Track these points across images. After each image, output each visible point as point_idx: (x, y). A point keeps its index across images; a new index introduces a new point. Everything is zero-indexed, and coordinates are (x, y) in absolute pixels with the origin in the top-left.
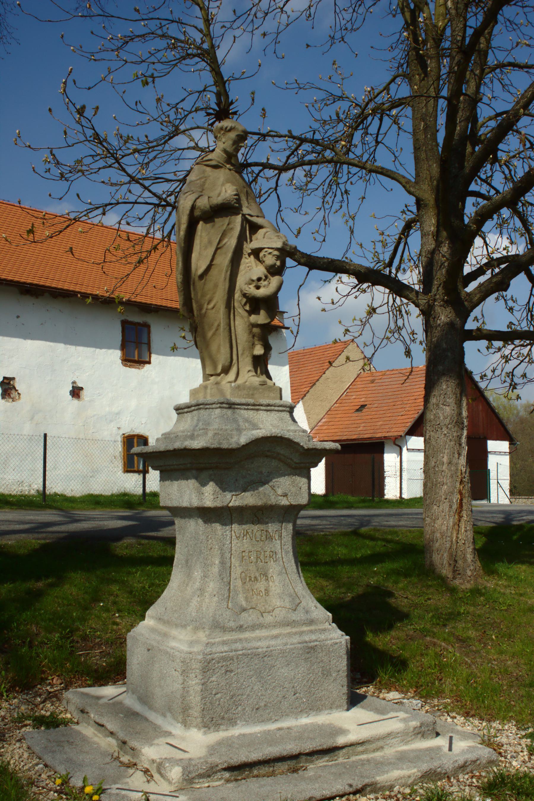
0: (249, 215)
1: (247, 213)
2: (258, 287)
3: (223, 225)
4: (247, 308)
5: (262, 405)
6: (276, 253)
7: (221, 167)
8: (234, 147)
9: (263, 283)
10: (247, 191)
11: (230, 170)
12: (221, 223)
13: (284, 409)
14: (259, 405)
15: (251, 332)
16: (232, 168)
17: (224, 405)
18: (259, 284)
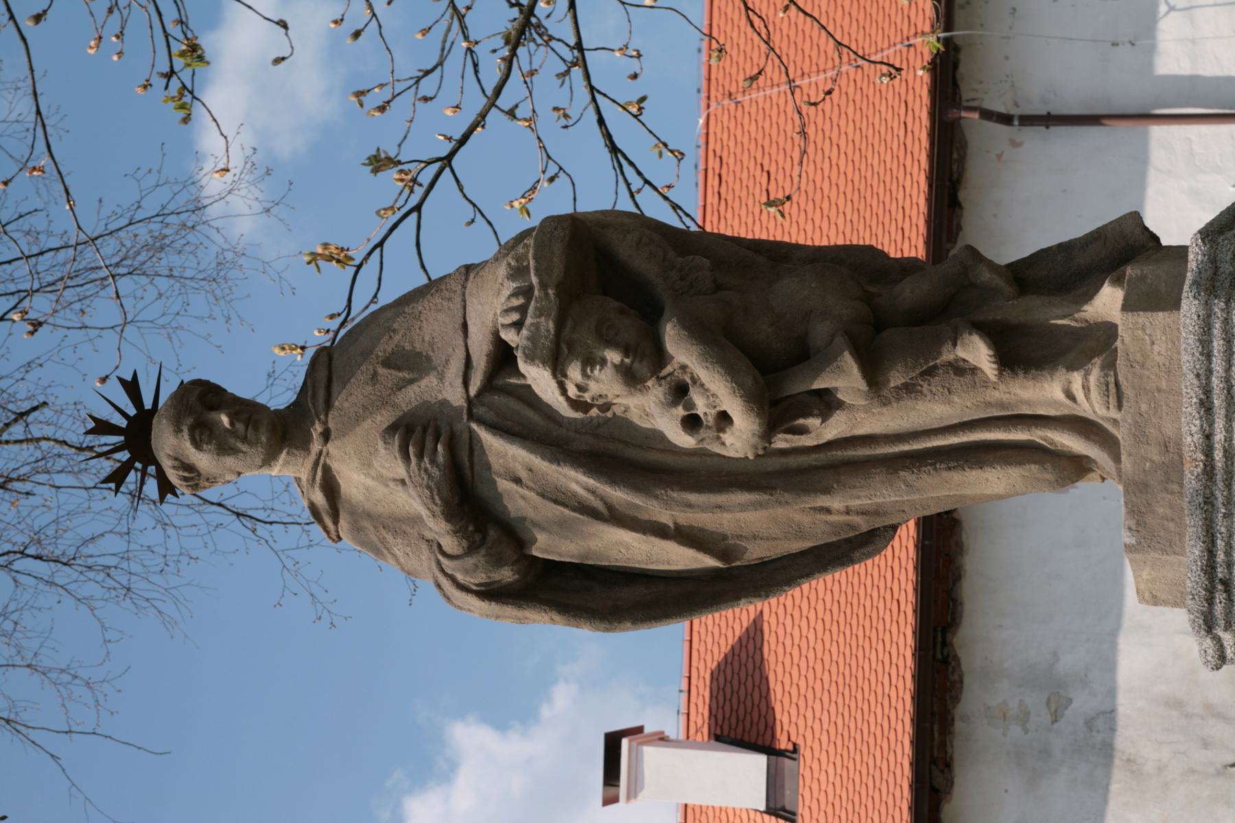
0: (466, 384)
1: (460, 389)
2: (724, 419)
3: (523, 497)
4: (813, 422)
5: (1208, 437)
6: (574, 372)
7: (327, 470)
8: (244, 448)
9: (701, 406)
10: (387, 363)
11: (326, 436)
12: (519, 501)
13: (1217, 330)
14: (1208, 452)
15: (909, 389)
16: (318, 427)
17: (1219, 609)
18: (710, 420)
